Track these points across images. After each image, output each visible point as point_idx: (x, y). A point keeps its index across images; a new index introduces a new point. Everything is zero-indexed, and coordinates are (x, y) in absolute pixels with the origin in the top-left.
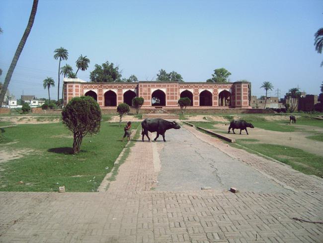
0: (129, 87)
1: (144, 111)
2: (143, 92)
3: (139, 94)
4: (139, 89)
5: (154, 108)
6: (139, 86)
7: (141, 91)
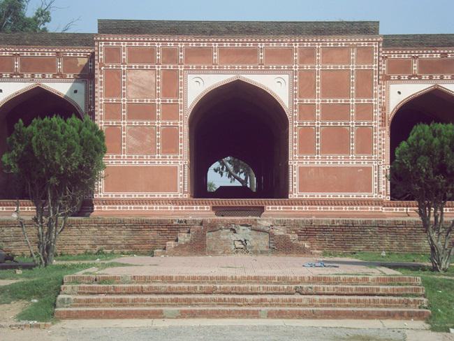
0: (30, 66)
1: (121, 237)
2: (130, 95)
3: (100, 111)
4: (99, 77)
5: (203, 211)
6: (101, 55)
7: (114, 87)
